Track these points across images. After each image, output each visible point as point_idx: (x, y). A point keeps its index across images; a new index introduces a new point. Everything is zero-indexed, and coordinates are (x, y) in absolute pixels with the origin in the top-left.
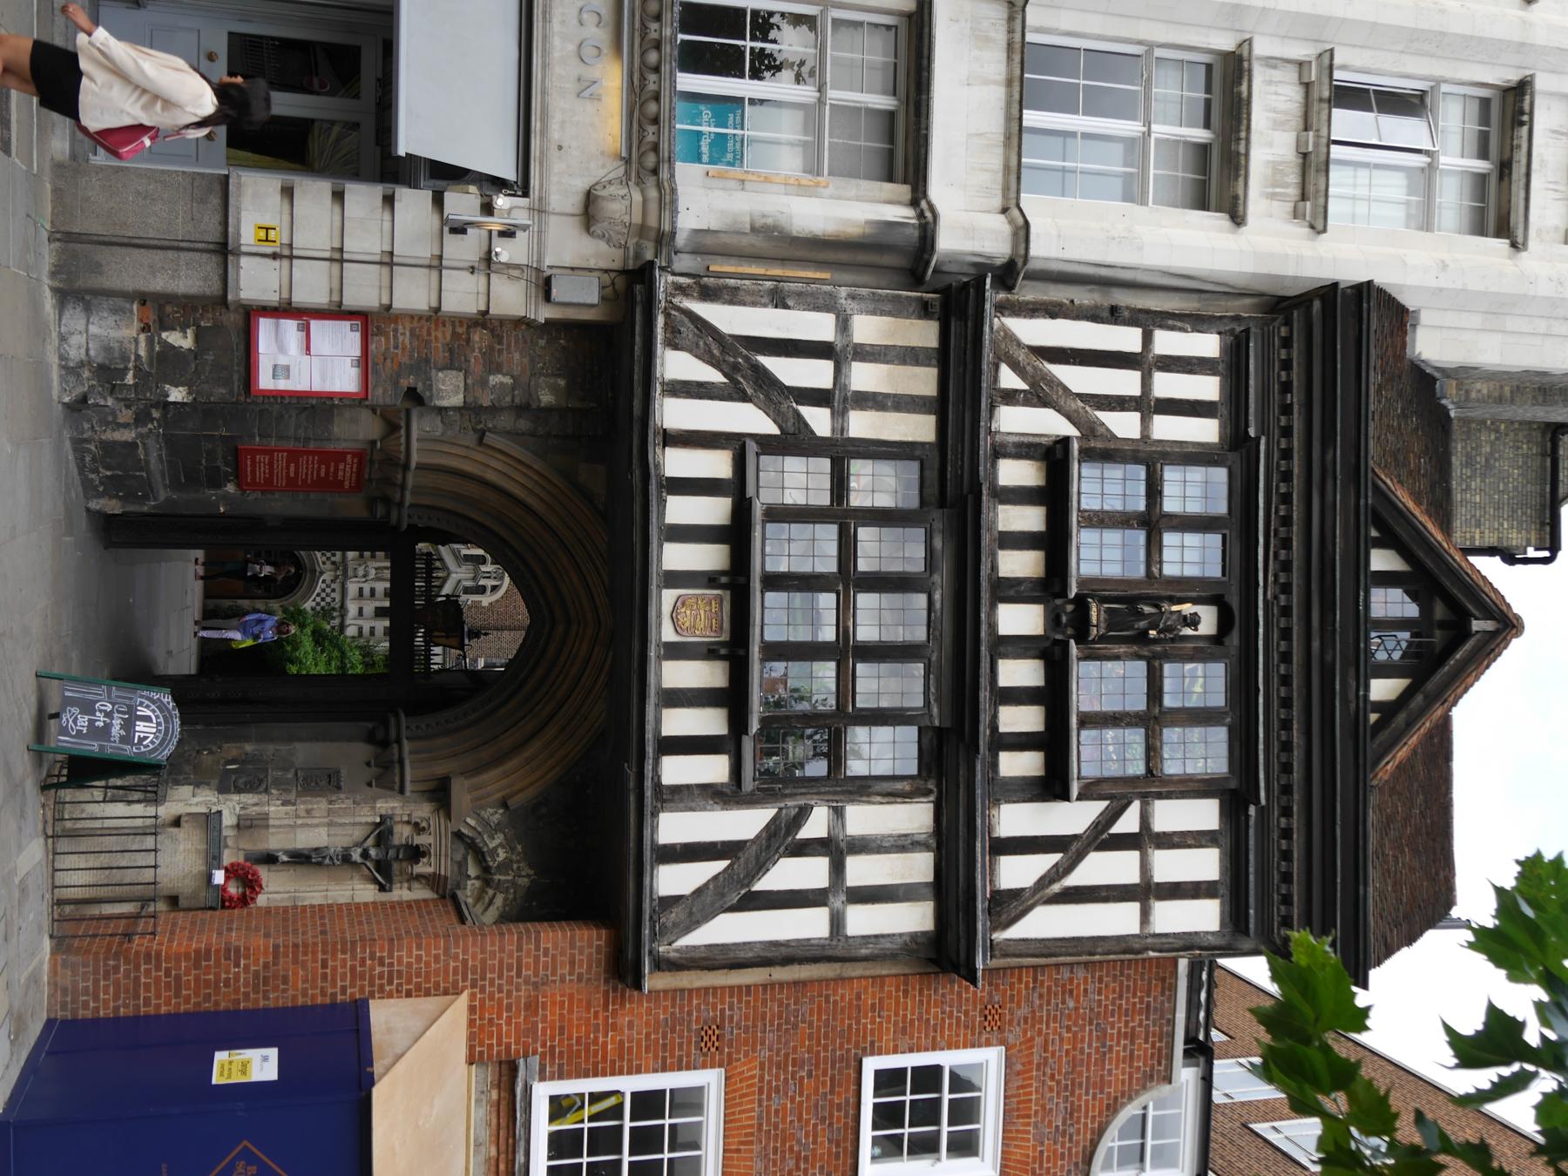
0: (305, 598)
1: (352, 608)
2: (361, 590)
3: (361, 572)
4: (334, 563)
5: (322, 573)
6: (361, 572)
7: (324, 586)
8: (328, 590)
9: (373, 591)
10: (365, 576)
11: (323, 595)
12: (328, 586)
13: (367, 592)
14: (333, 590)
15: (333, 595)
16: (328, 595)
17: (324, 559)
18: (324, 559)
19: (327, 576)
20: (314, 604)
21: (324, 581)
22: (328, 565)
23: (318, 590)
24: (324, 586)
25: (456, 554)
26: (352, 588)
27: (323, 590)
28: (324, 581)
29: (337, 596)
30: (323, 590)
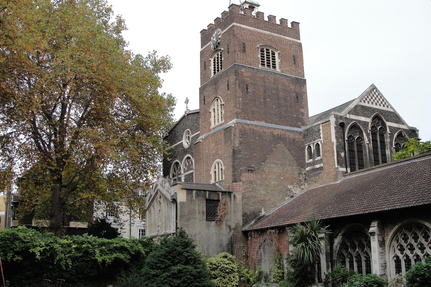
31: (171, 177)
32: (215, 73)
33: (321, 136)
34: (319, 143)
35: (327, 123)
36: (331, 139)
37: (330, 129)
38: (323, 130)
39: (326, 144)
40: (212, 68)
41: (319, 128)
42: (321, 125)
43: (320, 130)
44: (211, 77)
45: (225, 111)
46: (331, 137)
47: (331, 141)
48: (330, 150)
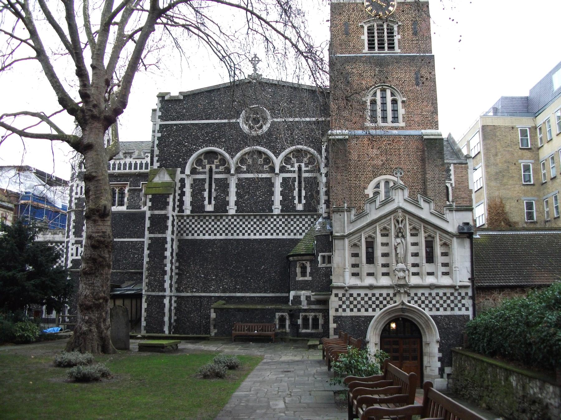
0: (421, 315)
1: (430, 280)
2: (414, 274)
3: (401, 274)
4: (395, 295)
5: (403, 303)
6: (401, 274)
7: (413, 302)
8: (416, 298)
9: (414, 265)
10: (404, 271)
11: (419, 302)
12: (413, 299)
13: (415, 270)
14: (416, 295)
15: (419, 295)
16: (420, 299)
17: (392, 302)
18: (392, 302)
19: (405, 300)
20: (427, 309)
21: (409, 302)
22: (397, 298)
23: (416, 306)
24: (413, 302)
25: (384, 203)
26: (414, 281)
27: (416, 302)
28: (409, 302)
29: (420, 292)
30: (416, 302)
31: (188, 171)
32: (371, 47)
33: (452, 177)
34: (448, 185)
35: (463, 165)
36: (468, 185)
37: (467, 173)
38: (455, 172)
39: (459, 189)
40: (365, 37)
41: (449, 167)
42: (452, 165)
43: (450, 170)
44: (364, 51)
45: (408, 112)
46: (468, 183)
47: (468, 187)
48: (467, 197)
